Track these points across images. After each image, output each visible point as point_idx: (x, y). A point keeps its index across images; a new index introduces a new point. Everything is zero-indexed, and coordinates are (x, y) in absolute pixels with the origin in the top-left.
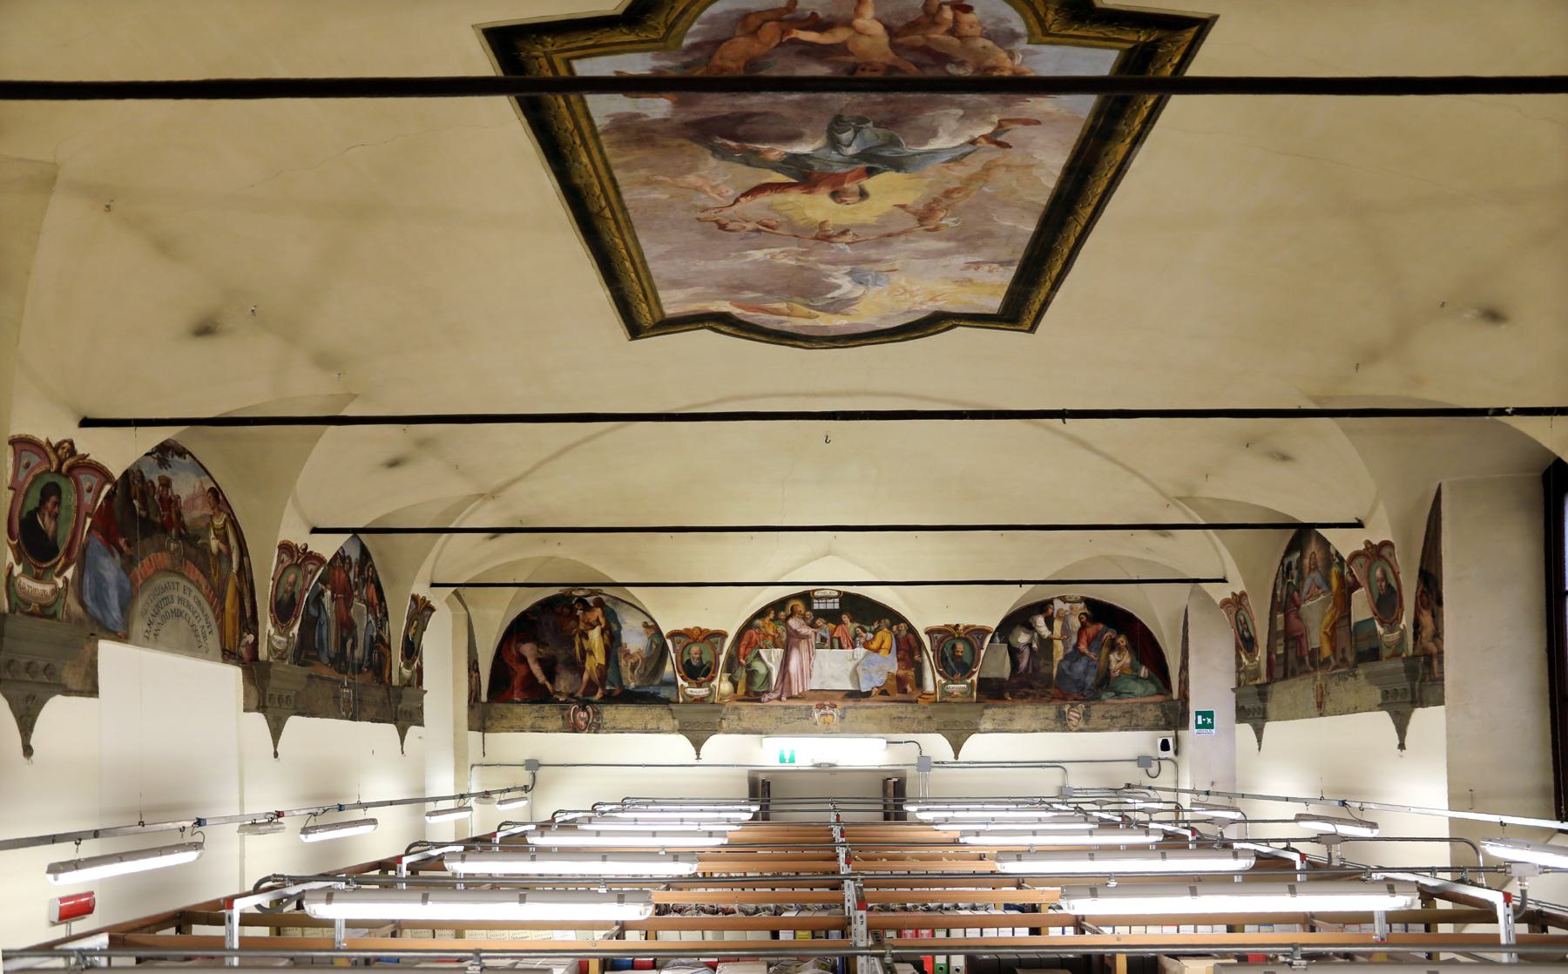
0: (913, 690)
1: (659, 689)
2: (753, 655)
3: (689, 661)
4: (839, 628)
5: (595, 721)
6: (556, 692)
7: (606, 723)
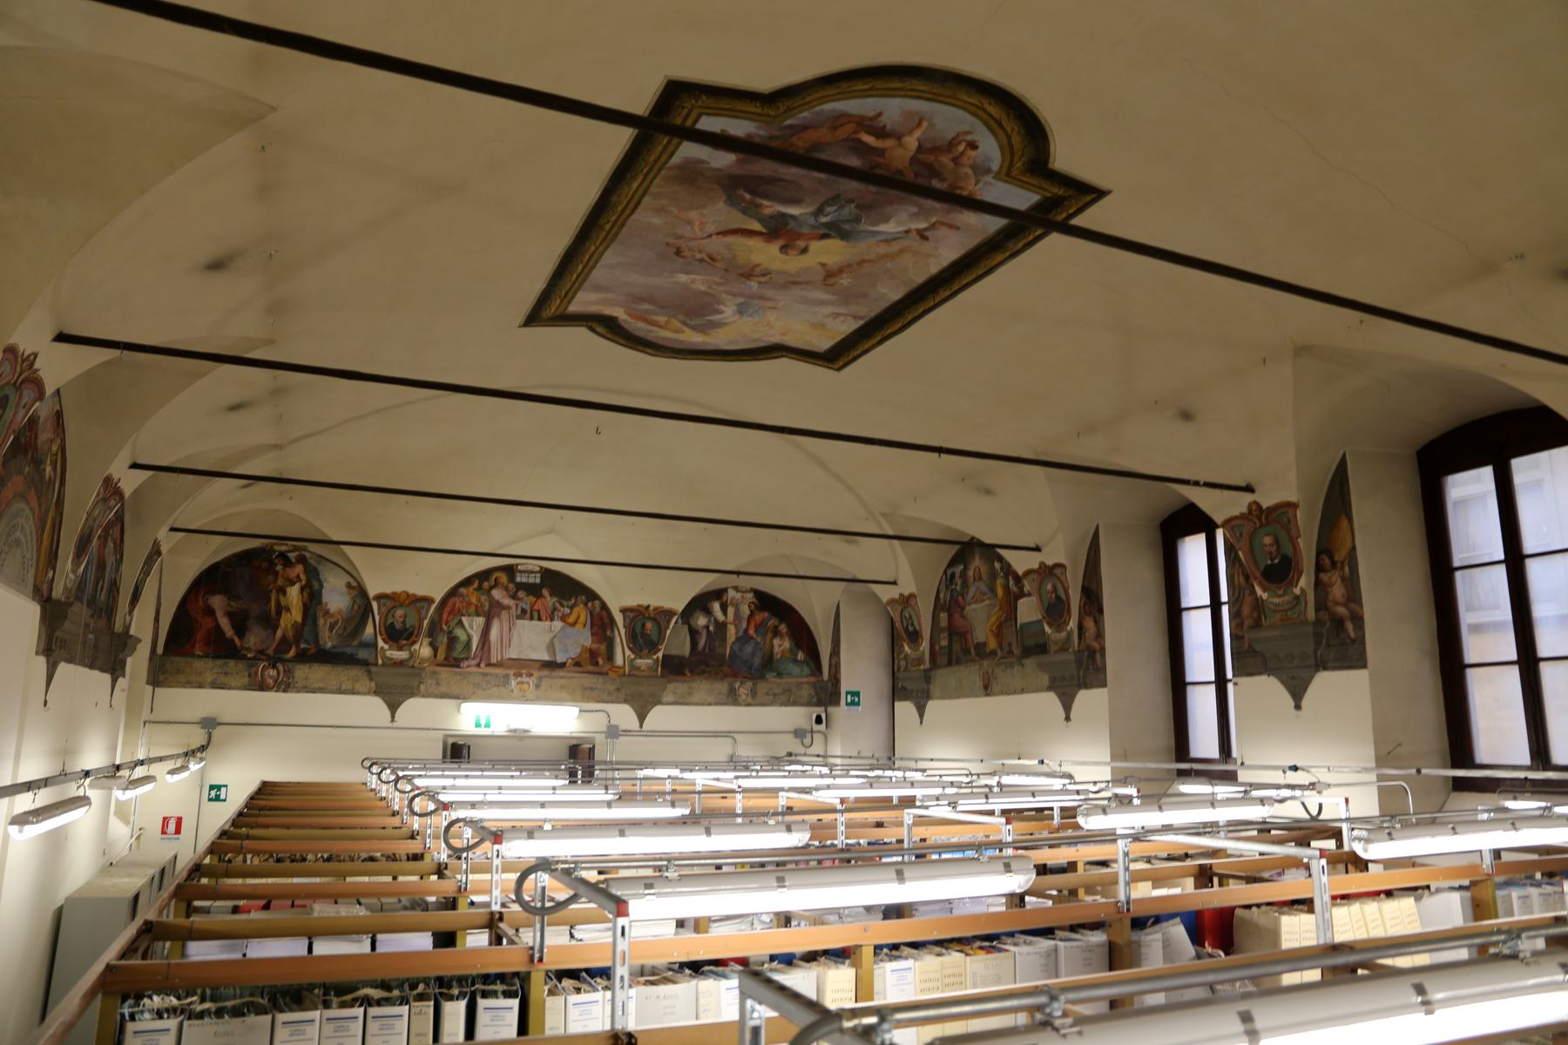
0: (604, 663)
2: (455, 622)
3: (392, 624)
4: (539, 602)
6: (243, 648)
7: (297, 682)
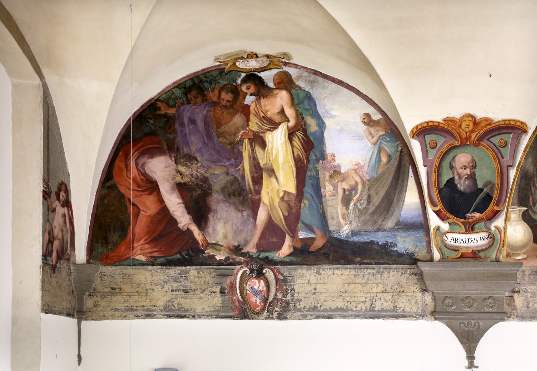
1: (395, 236)
3: (451, 182)
5: (280, 296)
6: (208, 245)
7: (300, 301)
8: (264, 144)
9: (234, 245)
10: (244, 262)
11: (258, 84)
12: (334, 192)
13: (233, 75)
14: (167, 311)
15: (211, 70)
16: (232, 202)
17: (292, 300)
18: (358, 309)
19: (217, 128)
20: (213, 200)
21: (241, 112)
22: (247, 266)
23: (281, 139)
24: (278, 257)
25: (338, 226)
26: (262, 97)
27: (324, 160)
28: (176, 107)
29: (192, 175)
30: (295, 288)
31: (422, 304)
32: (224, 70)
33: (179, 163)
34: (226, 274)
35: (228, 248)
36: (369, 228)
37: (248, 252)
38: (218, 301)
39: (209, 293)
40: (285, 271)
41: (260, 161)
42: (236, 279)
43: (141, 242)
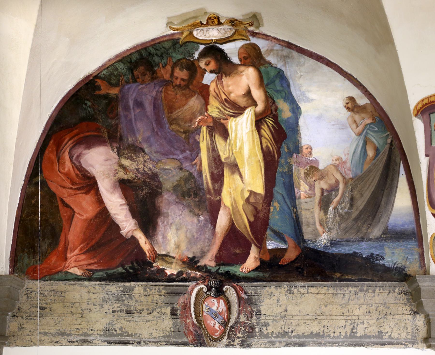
1: (382, 247)
5: (243, 319)
6: (157, 256)
7: (267, 325)
8: (225, 133)
9: (188, 257)
10: (200, 278)
11: (219, 59)
12: (310, 192)
13: (190, 46)
14: (107, 336)
15: (162, 40)
16: (187, 204)
17: (258, 324)
18: (336, 335)
19: (168, 113)
20: (164, 202)
21: (198, 94)
22: (204, 282)
23: (246, 128)
24: (242, 272)
25: (314, 234)
26: (224, 76)
27: (299, 153)
28: (119, 86)
29: (137, 170)
30: (261, 309)
31: (413, 329)
32: (178, 41)
33: (123, 155)
34: (179, 291)
35: (181, 261)
36: (352, 237)
37: (205, 266)
38: (168, 324)
39: (158, 315)
40: (250, 289)
41: (221, 154)
42: (190, 298)
43: (76, 252)
